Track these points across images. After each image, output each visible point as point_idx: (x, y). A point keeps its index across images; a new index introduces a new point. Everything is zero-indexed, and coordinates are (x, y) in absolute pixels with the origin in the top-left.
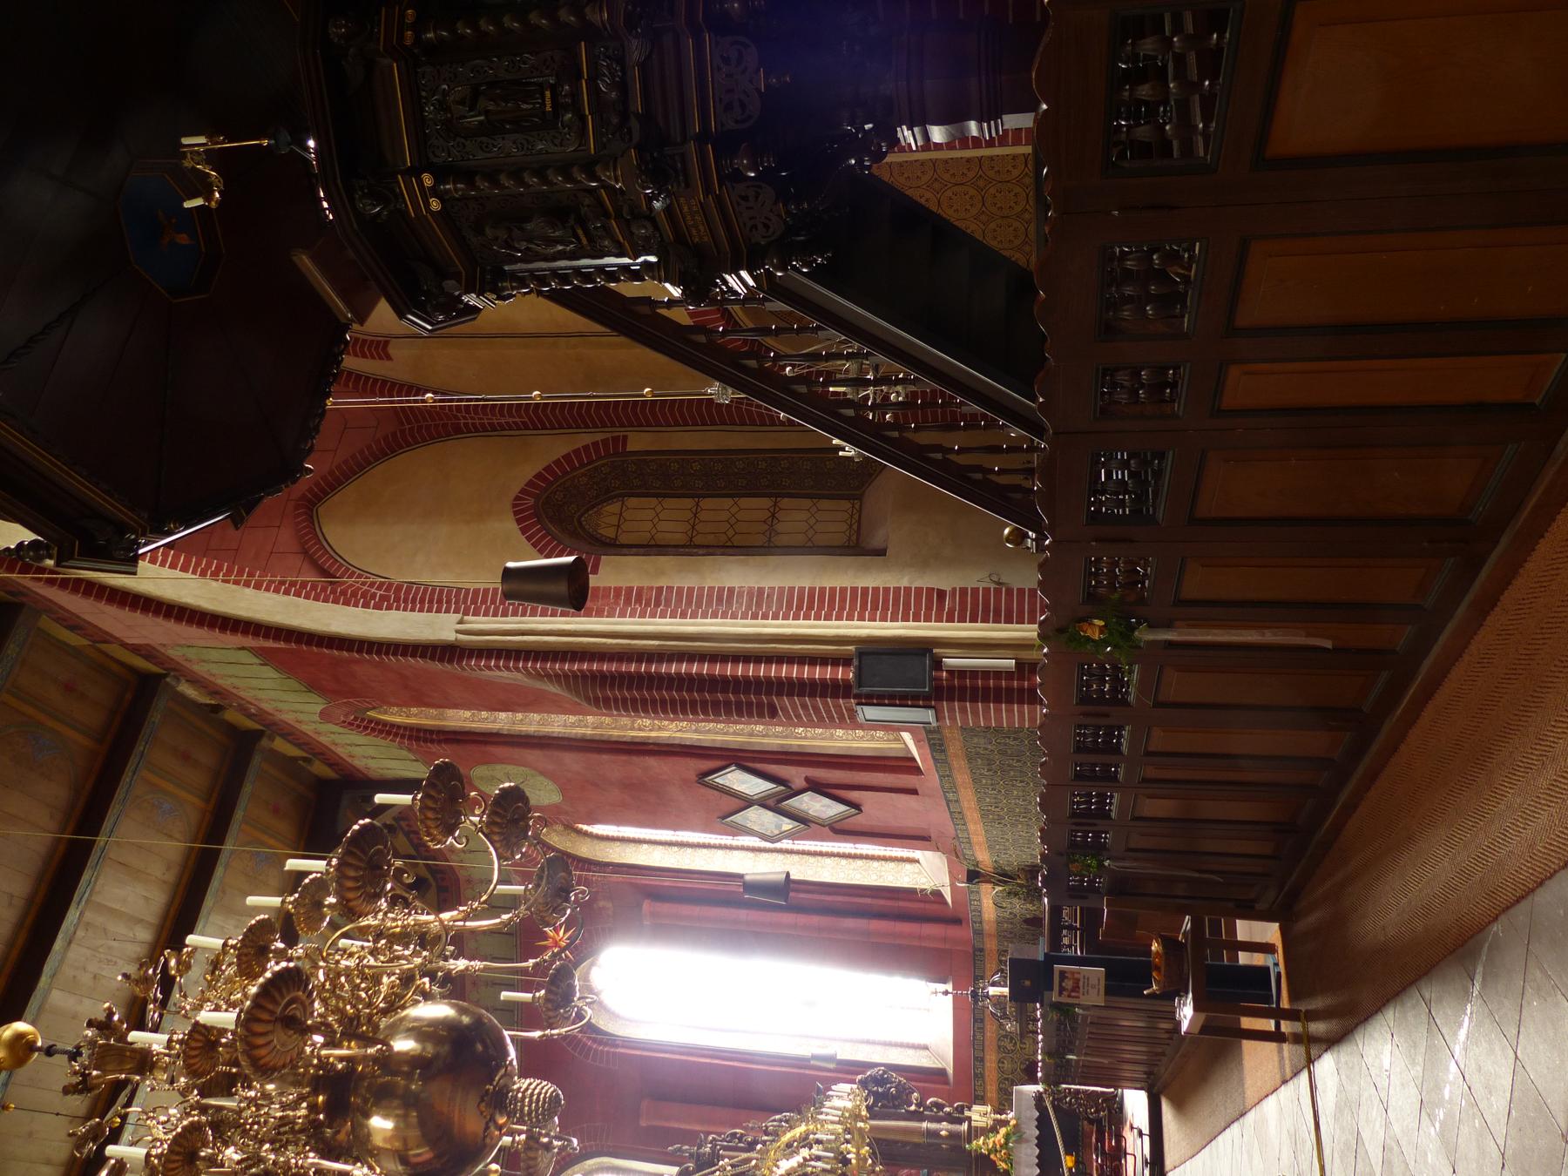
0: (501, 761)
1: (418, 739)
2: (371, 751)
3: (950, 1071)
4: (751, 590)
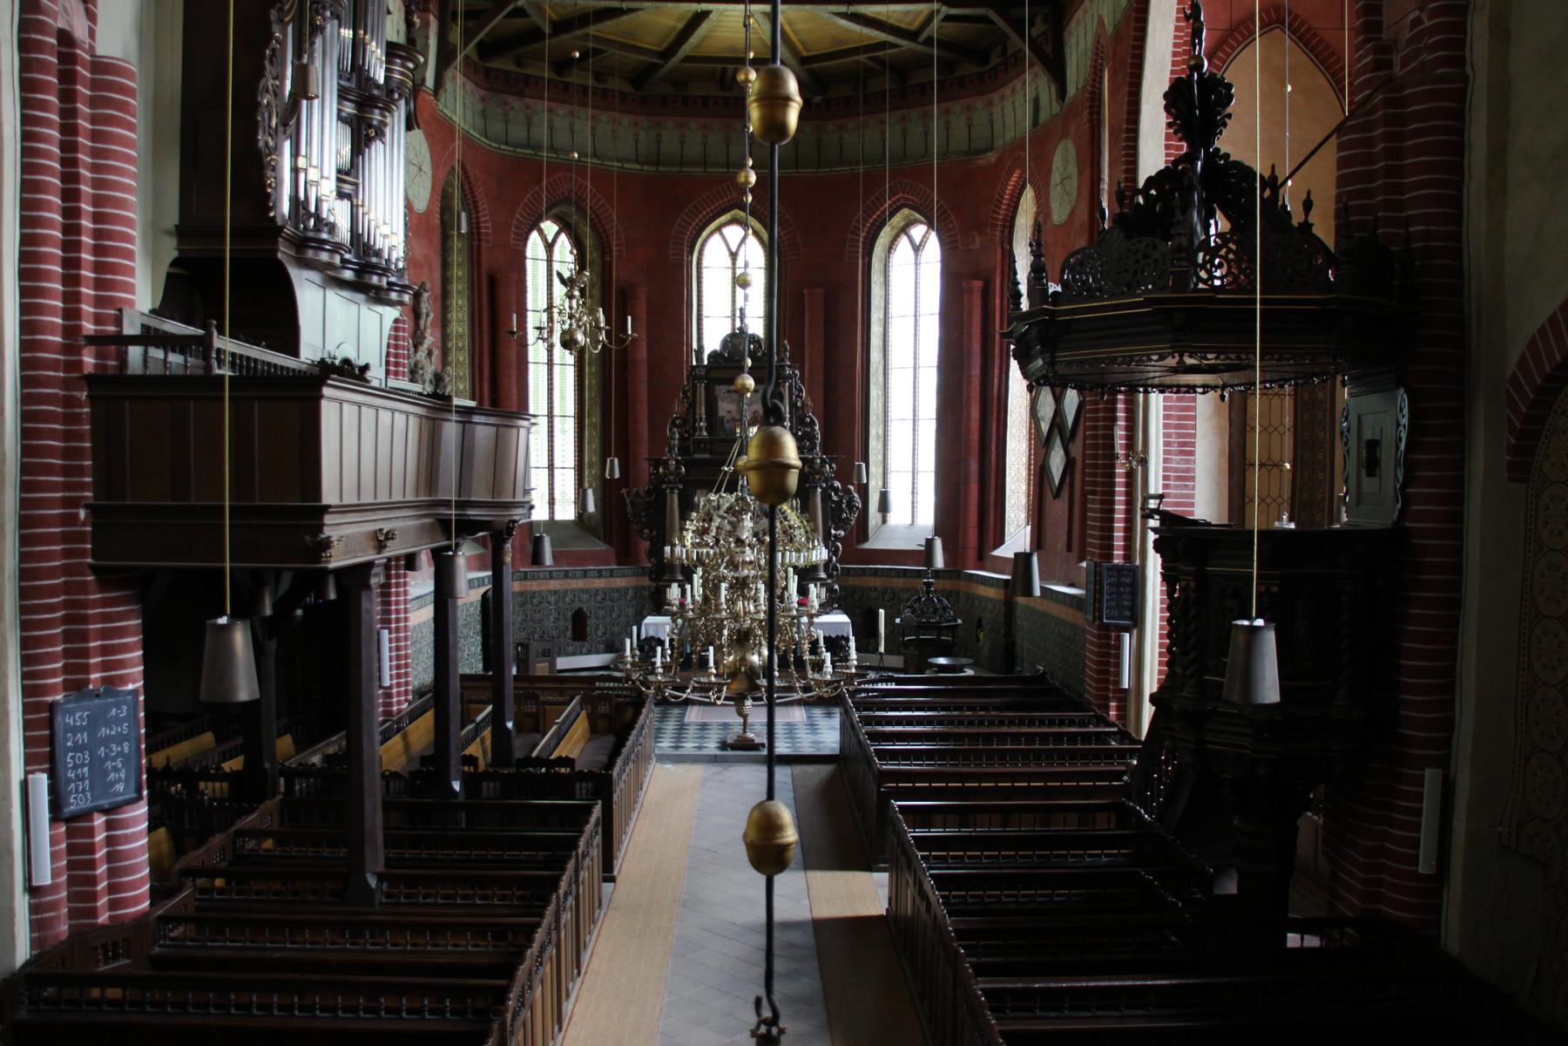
0: (1080, 174)
1: (1092, 99)
2: (1082, 45)
3: (867, 546)
4: (1193, 470)
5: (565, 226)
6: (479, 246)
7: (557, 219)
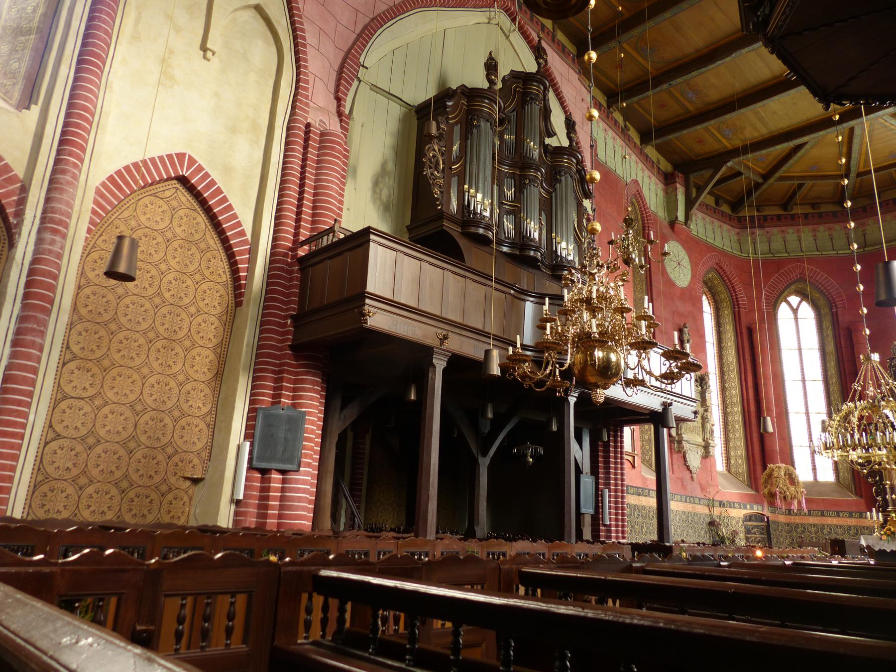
5: (804, 296)
6: (739, 311)
7: (798, 293)
